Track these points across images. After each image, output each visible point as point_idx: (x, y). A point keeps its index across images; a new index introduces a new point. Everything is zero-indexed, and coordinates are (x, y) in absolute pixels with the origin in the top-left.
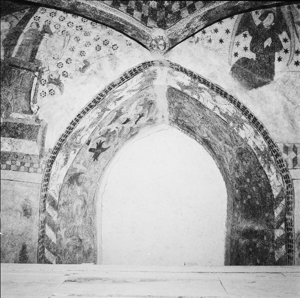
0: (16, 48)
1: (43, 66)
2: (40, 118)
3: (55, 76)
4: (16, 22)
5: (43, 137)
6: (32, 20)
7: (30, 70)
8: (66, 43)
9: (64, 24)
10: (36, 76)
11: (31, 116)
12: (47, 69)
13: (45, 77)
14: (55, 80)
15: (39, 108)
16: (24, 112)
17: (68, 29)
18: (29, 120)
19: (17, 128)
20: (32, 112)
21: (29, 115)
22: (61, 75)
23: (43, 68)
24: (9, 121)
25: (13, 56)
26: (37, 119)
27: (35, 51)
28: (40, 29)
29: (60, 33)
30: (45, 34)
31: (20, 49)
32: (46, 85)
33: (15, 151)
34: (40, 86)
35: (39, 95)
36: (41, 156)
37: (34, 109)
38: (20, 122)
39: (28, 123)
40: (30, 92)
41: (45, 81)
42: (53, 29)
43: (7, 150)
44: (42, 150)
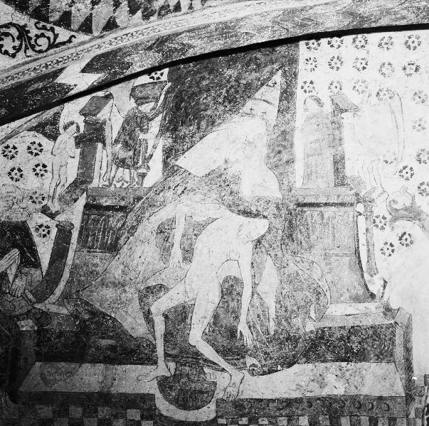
0: (299, 167)
1: (369, 188)
2: (394, 306)
3: (404, 201)
4: (272, 111)
5: (408, 350)
6: (299, 94)
7: (342, 204)
8: (398, 115)
9: (372, 74)
10: (360, 214)
11: (372, 306)
12: (380, 190)
13: (380, 209)
14: (406, 209)
15: (385, 282)
16: (357, 299)
17: (388, 83)
18: (369, 314)
19: (348, 338)
20: (373, 296)
21: (366, 304)
22: (417, 193)
23: (370, 192)
24: (327, 324)
25: (298, 185)
26: (388, 310)
27: (338, 163)
28: (328, 108)
29: (374, 99)
30: (343, 115)
31: (307, 165)
32: (388, 228)
33: (353, 392)
34: (376, 231)
35: (377, 253)
36: (409, 398)
37: (375, 288)
38: (350, 322)
39: (368, 322)
40: (357, 252)
41: (384, 218)
42: (354, 98)
43: (335, 392)
44: (409, 384)
